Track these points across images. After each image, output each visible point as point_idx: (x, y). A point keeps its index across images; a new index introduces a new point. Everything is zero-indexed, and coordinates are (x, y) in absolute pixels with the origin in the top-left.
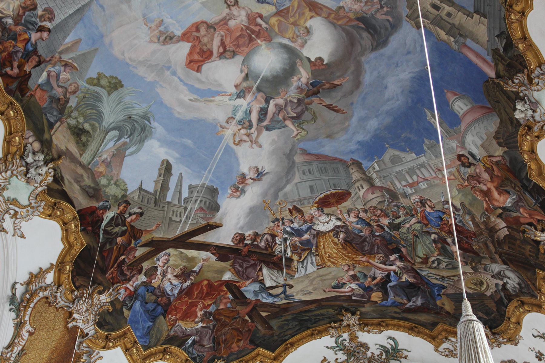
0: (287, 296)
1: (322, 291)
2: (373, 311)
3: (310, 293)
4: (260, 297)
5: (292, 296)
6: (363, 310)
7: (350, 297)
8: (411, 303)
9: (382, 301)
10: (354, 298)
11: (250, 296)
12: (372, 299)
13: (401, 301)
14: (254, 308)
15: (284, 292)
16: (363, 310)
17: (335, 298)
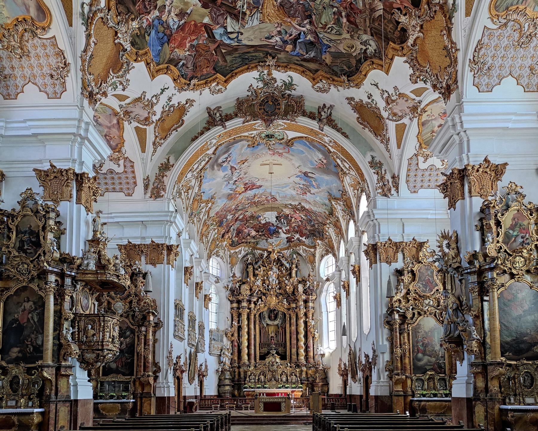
0: (238, 40)
1: (259, 40)
2: (285, 58)
3: (252, 40)
4: (223, 39)
5: (241, 41)
6: (279, 56)
7: (274, 46)
8: (307, 55)
9: (291, 51)
10: (276, 47)
11: (217, 37)
12: (286, 50)
13: (302, 53)
14: (218, 46)
15: (237, 37)
16: (279, 56)
17: (265, 46)
